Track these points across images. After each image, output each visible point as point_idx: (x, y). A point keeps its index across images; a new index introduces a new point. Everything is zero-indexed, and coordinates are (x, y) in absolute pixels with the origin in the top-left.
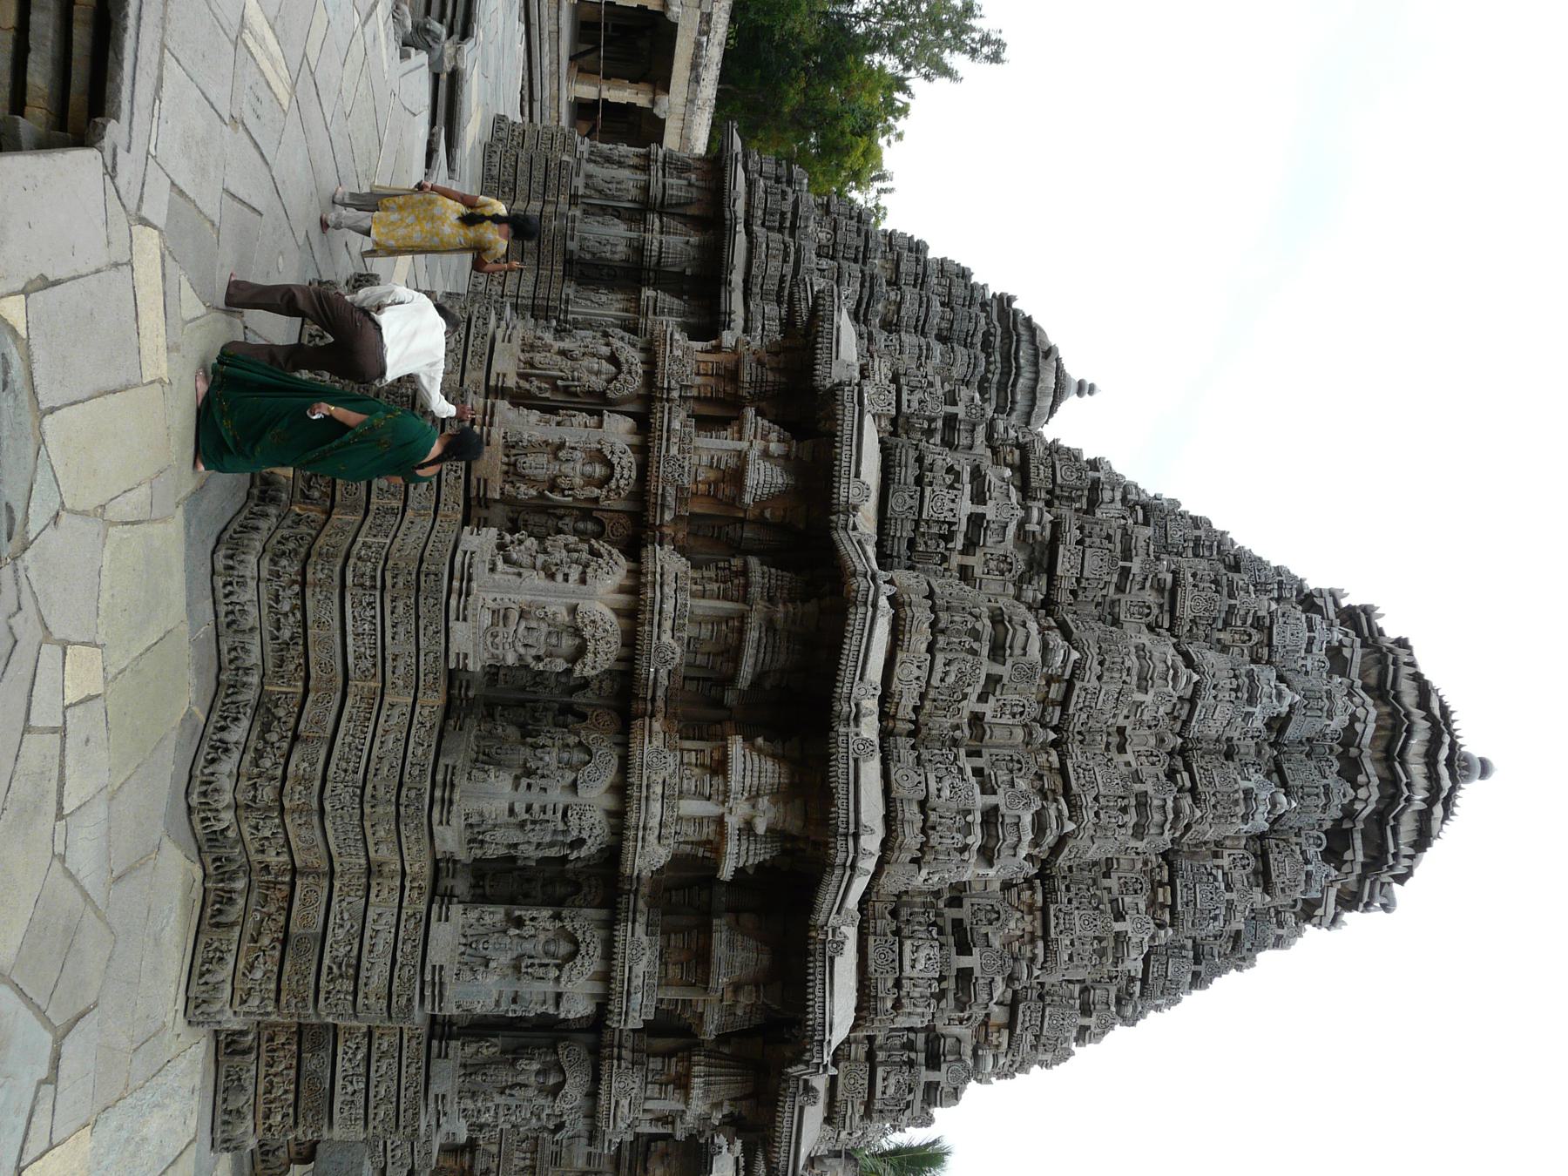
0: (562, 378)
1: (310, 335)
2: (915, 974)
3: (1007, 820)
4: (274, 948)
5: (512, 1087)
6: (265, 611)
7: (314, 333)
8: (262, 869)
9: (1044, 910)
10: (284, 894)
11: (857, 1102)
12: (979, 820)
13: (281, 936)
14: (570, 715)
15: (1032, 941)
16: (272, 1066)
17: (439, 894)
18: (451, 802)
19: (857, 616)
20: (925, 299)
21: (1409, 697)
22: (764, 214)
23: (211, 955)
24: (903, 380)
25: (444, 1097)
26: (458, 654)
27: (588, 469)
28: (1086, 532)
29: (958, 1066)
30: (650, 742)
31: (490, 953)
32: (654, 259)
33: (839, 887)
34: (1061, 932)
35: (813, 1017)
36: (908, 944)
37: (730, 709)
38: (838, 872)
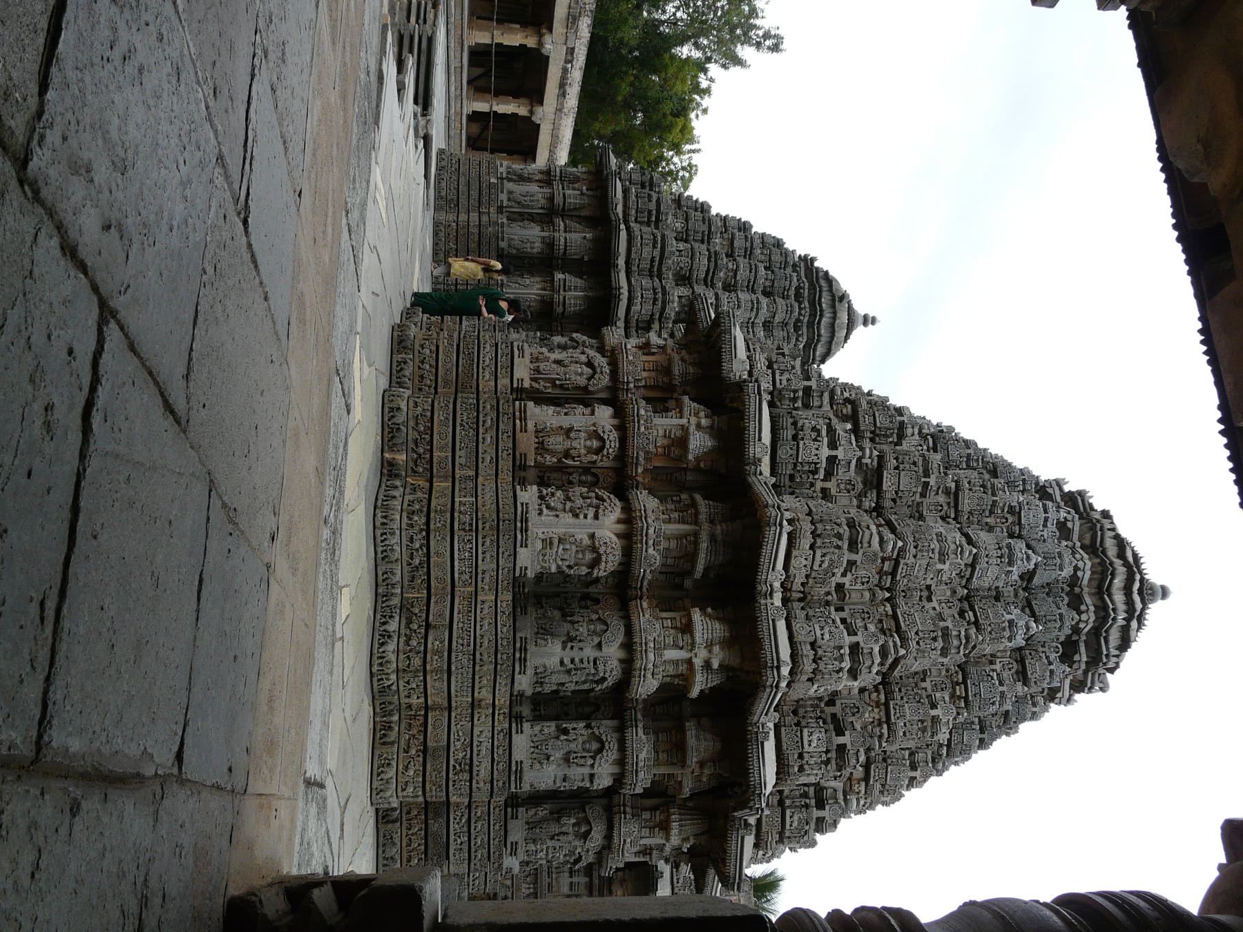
0: (558, 379)
1: (397, 361)
2: (811, 749)
3: (865, 651)
4: (419, 756)
5: (558, 835)
6: (404, 549)
7: (400, 360)
8: (406, 708)
9: (887, 705)
10: (421, 722)
11: (774, 832)
12: (848, 652)
13: (422, 748)
14: (589, 601)
15: (880, 724)
16: (410, 829)
17: (515, 718)
18: (525, 660)
19: (771, 533)
20: (753, 267)
21: (1112, 551)
22: (636, 212)
23: (383, 762)
24: (775, 366)
25: (516, 843)
26: (521, 568)
27: (588, 443)
28: (900, 460)
29: (836, 807)
30: (644, 615)
31: (550, 752)
32: (562, 251)
33: (768, 699)
34: (898, 718)
35: (753, 779)
36: (805, 731)
37: (687, 590)
38: (768, 690)
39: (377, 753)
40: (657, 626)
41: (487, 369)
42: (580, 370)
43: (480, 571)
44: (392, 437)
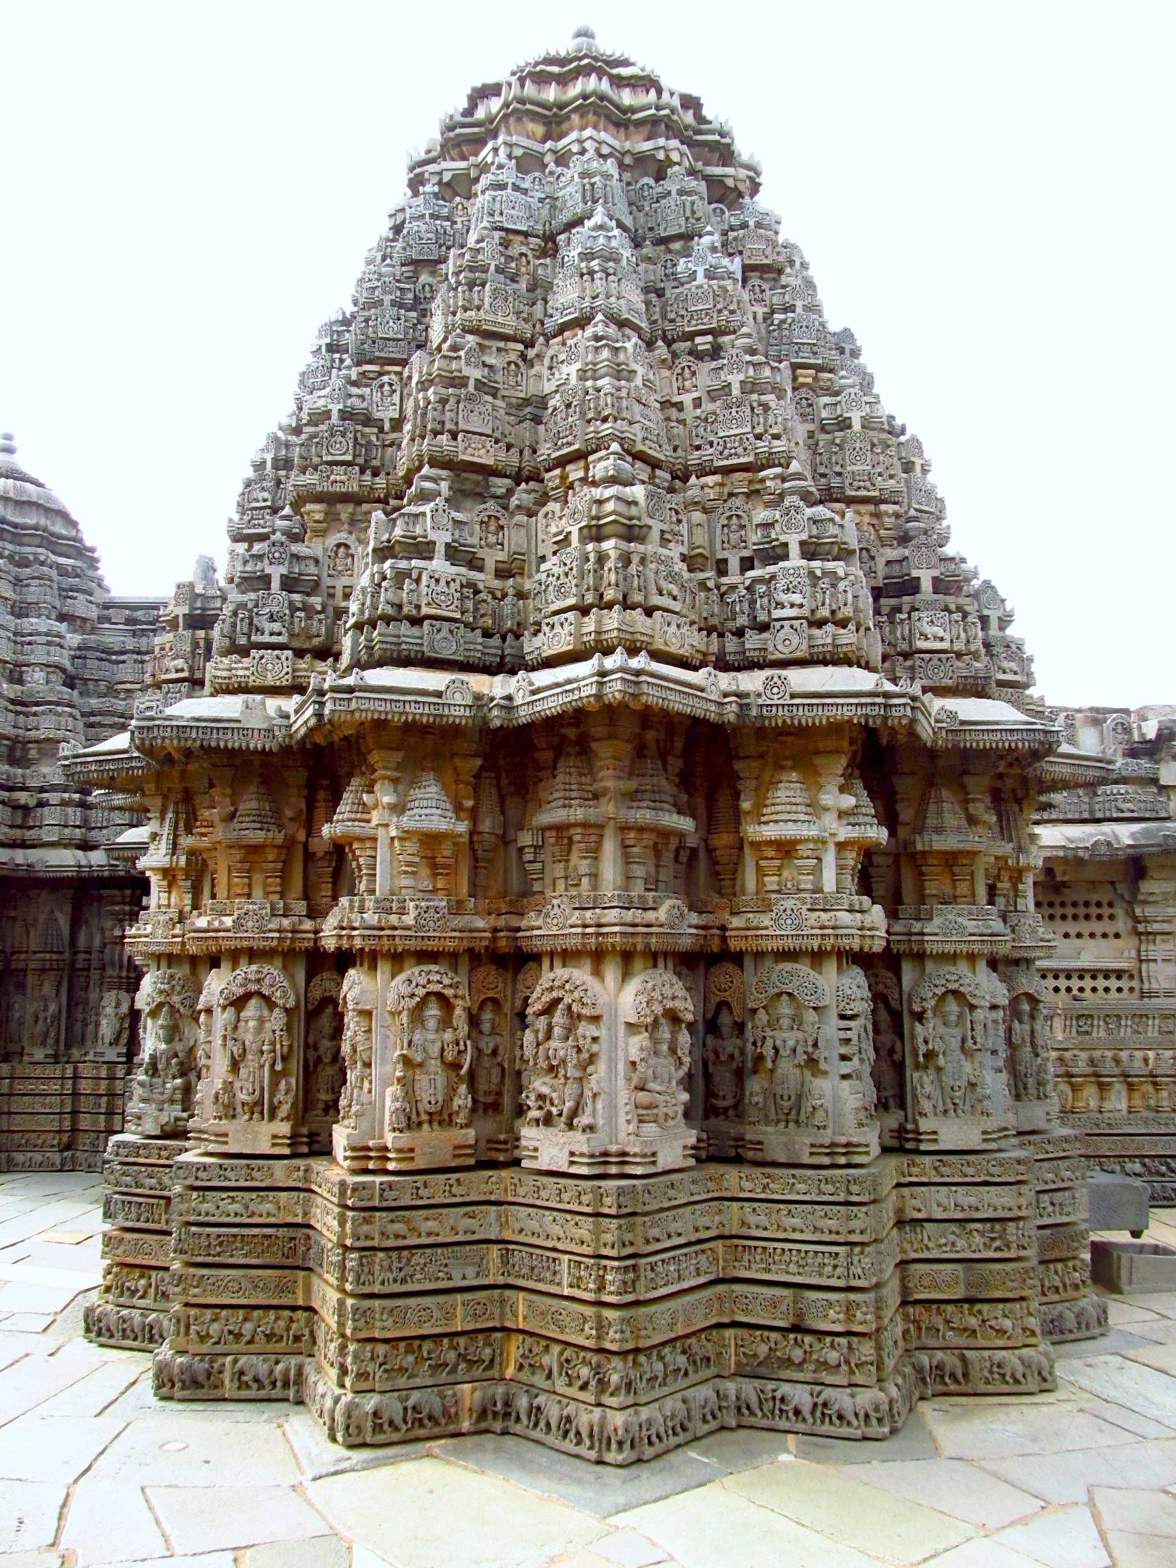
0: (273, 1065)
1: (239, 1388)
3: (814, 532)
4: (979, 1312)
6: (666, 1390)
7: (236, 1384)
13: (966, 1306)
19: (652, 696)
23: (996, 1376)
24: (243, 641)
28: (439, 427)
30: (766, 928)
36: (922, 644)
39: (983, 1388)
40: (789, 904)
41: (252, 1207)
42: (252, 1024)
43: (694, 1237)
44: (430, 1418)
